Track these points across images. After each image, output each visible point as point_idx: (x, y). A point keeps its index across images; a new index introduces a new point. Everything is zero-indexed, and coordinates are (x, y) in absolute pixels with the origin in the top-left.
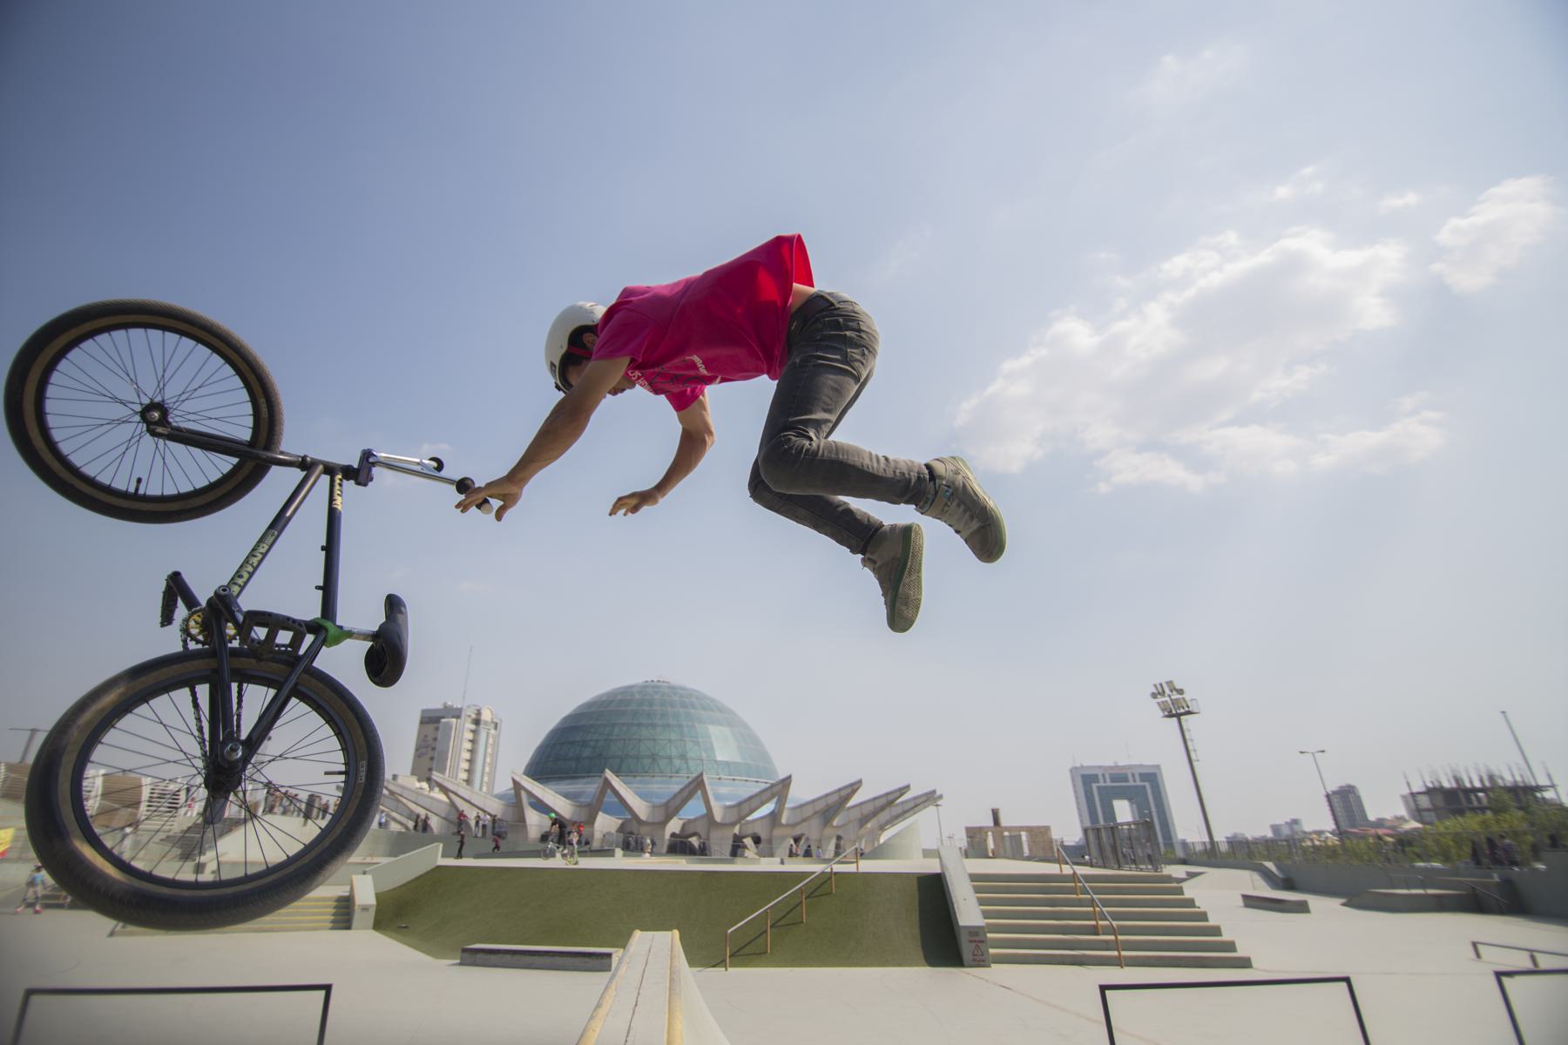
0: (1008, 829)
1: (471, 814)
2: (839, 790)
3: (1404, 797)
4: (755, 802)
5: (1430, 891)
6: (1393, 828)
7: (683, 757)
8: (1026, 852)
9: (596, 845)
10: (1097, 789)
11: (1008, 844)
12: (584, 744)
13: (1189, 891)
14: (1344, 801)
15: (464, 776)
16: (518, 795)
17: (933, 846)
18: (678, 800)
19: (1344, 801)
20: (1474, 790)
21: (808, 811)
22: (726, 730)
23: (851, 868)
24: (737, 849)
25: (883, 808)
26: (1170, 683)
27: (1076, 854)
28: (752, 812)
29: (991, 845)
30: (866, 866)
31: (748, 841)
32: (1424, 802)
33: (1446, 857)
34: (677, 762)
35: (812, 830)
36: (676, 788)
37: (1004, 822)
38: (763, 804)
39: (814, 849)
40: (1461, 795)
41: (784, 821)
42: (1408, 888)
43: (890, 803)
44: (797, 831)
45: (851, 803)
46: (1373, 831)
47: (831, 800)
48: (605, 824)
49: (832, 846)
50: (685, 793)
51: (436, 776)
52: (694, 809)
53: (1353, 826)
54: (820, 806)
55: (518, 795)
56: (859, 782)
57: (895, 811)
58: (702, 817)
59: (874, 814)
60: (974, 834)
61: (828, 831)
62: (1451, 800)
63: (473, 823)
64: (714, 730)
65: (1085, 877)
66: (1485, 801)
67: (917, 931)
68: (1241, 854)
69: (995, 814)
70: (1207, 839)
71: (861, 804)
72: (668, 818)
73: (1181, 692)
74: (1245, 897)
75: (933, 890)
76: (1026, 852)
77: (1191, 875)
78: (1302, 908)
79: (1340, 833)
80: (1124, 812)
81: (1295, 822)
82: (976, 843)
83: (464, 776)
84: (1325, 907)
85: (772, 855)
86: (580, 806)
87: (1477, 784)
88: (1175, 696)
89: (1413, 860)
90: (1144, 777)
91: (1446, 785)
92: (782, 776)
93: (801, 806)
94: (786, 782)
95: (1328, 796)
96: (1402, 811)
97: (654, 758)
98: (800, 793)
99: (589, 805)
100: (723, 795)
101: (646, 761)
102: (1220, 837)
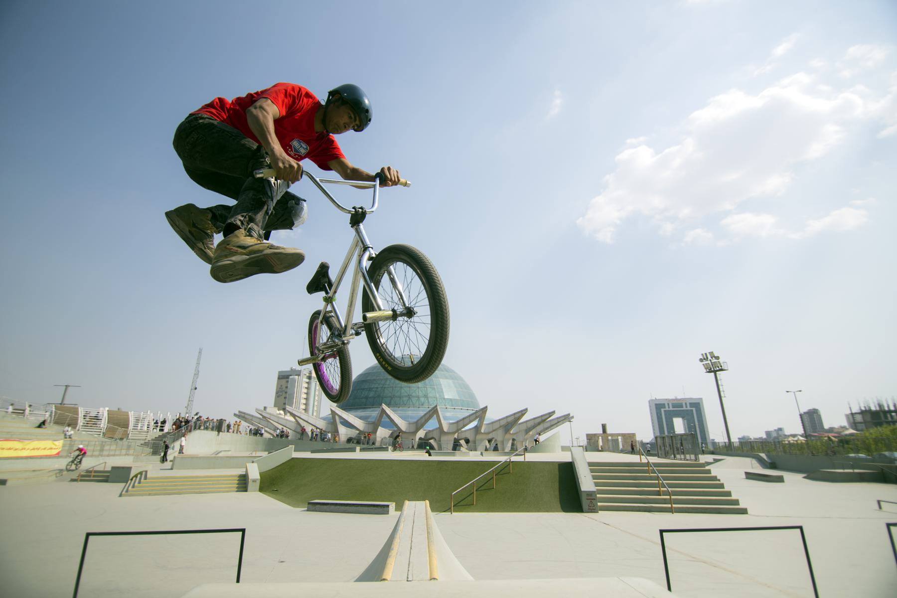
0: (612, 435)
1: (309, 429)
3: (847, 416)
4: (466, 421)
5: (856, 471)
6: (839, 433)
7: (426, 396)
8: (621, 447)
9: (377, 444)
10: (663, 412)
11: (610, 443)
12: (370, 390)
13: (716, 470)
14: (811, 418)
15: (303, 407)
16: (334, 418)
17: (568, 444)
18: (423, 420)
19: (811, 418)
20: (890, 412)
21: (497, 426)
22: (451, 381)
23: (520, 459)
24: (456, 446)
25: (539, 424)
26: (711, 353)
27: (649, 449)
28: (464, 426)
29: (600, 443)
30: (531, 457)
31: (462, 442)
32: (859, 418)
33: (868, 450)
34: (422, 399)
35: (498, 436)
36: (422, 413)
37: (609, 431)
38: (471, 422)
39: (499, 448)
40: (882, 415)
41: (482, 431)
42: (844, 469)
43: (543, 421)
44: (490, 436)
45: (522, 420)
46: (826, 434)
47: (510, 419)
48: (382, 433)
49: (509, 445)
51: (288, 408)
52: (432, 425)
53: (815, 432)
54: (503, 423)
55: (334, 418)
56: (526, 409)
57: (546, 425)
59: (534, 427)
60: (591, 438)
61: (508, 436)
62: (876, 417)
63: (310, 434)
64: (442, 381)
65: (654, 464)
66: (895, 417)
67: (557, 493)
68: (746, 448)
69: (604, 427)
70: (727, 441)
72: (417, 430)
73: (717, 358)
74: (746, 473)
75: (567, 471)
76: (621, 447)
77: (716, 461)
78: (780, 479)
79: (806, 435)
80: (679, 425)
81: (780, 429)
82: (592, 444)
83: (303, 407)
84: (794, 481)
85: (476, 450)
86: (369, 423)
87: (892, 408)
88: (714, 360)
89: (849, 453)
90: (692, 405)
91: (873, 408)
92: (482, 407)
93: (493, 423)
94: (485, 409)
95: (801, 415)
96: (844, 423)
97: (409, 397)
98: (493, 415)
99: (373, 423)
100: (448, 417)
102: (735, 439)
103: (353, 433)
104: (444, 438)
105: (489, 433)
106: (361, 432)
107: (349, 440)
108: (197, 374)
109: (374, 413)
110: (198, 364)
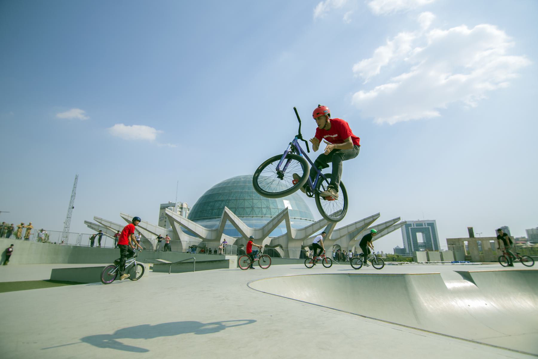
2: (364, 220)
21: (345, 232)
36: (265, 222)
41: (330, 238)
47: (359, 225)
50: (271, 226)
54: (351, 229)
58: (283, 236)
71: (378, 225)
101: (248, 210)
103: (196, 241)
104: (291, 245)
105: (335, 240)
106: (204, 240)
107: (193, 248)
108: (73, 196)
109: (216, 223)
110: (75, 187)
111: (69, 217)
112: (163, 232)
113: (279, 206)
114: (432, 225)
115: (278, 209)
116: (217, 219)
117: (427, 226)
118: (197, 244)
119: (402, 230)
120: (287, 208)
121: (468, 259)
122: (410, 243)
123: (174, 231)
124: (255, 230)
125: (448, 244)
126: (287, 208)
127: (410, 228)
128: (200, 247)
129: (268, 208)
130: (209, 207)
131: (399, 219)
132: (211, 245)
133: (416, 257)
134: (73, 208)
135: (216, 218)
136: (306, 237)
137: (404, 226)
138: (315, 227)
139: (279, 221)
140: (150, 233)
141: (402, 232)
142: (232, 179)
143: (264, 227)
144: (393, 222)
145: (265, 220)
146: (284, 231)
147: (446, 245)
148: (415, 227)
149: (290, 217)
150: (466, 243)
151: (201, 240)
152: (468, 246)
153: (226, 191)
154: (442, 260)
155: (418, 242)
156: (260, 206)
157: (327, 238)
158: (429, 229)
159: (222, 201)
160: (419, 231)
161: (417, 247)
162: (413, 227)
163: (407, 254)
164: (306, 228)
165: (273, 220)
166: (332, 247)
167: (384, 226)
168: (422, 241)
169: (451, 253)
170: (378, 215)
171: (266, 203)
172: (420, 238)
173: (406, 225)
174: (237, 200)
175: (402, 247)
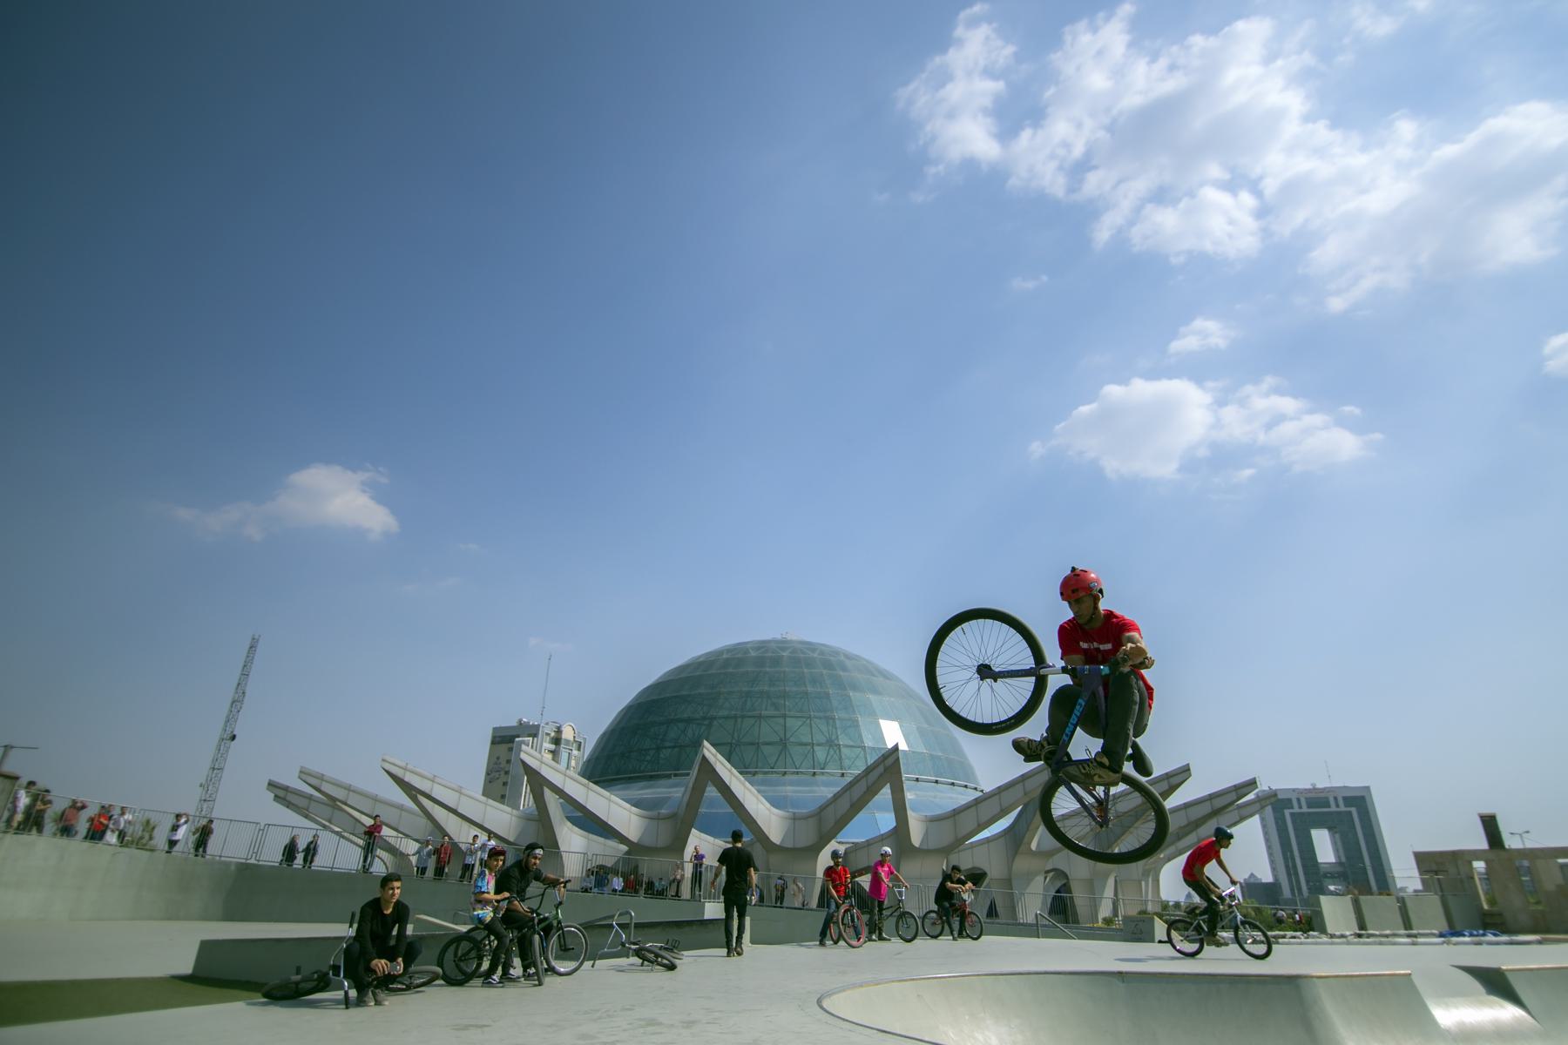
36: (828, 792)
41: (1034, 846)
50: (844, 805)
71: (1187, 806)
101: (767, 750)
103: (609, 852)
107: (599, 876)
108: (237, 702)
109: (674, 792)
110: (245, 674)
111: (216, 768)
112: (504, 820)
113: (868, 743)
114: (1359, 802)
115: (864, 748)
116: (674, 780)
117: (1342, 808)
118: (609, 863)
119: (1262, 820)
120: (896, 748)
121: (1493, 922)
122: (1295, 866)
123: (541, 817)
124: (795, 818)
125: (1422, 871)
126: (896, 748)
127: (1287, 812)
128: (614, 871)
129: (831, 744)
130: (652, 738)
131: (1251, 784)
132: (650, 868)
133: (1319, 914)
134: (234, 738)
135: (669, 776)
136: (958, 843)
137: (1269, 809)
138: (987, 810)
139: (872, 791)
140: (466, 825)
141: (1264, 826)
142: (719, 653)
143: (823, 808)
144: (1233, 796)
145: (826, 784)
146: (887, 821)
147: (1416, 873)
148: (1305, 809)
149: (904, 776)
150: (1479, 865)
151: (624, 848)
152: (1489, 876)
153: (702, 690)
154: (1408, 925)
155: (1320, 860)
156: (807, 739)
157: (1022, 848)
158: (1351, 814)
159: (689, 721)
160: (1319, 826)
161: (1317, 878)
162: (1296, 810)
163: (1287, 902)
164: (956, 813)
165: (851, 785)
166: (1040, 878)
167: (1206, 809)
168: (1333, 860)
169: (1434, 900)
170: (1185, 772)
171: (824, 728)
172: (1325, 847)
173: (1276, 803)
174: (735, 717)
175: (1266, 876)
